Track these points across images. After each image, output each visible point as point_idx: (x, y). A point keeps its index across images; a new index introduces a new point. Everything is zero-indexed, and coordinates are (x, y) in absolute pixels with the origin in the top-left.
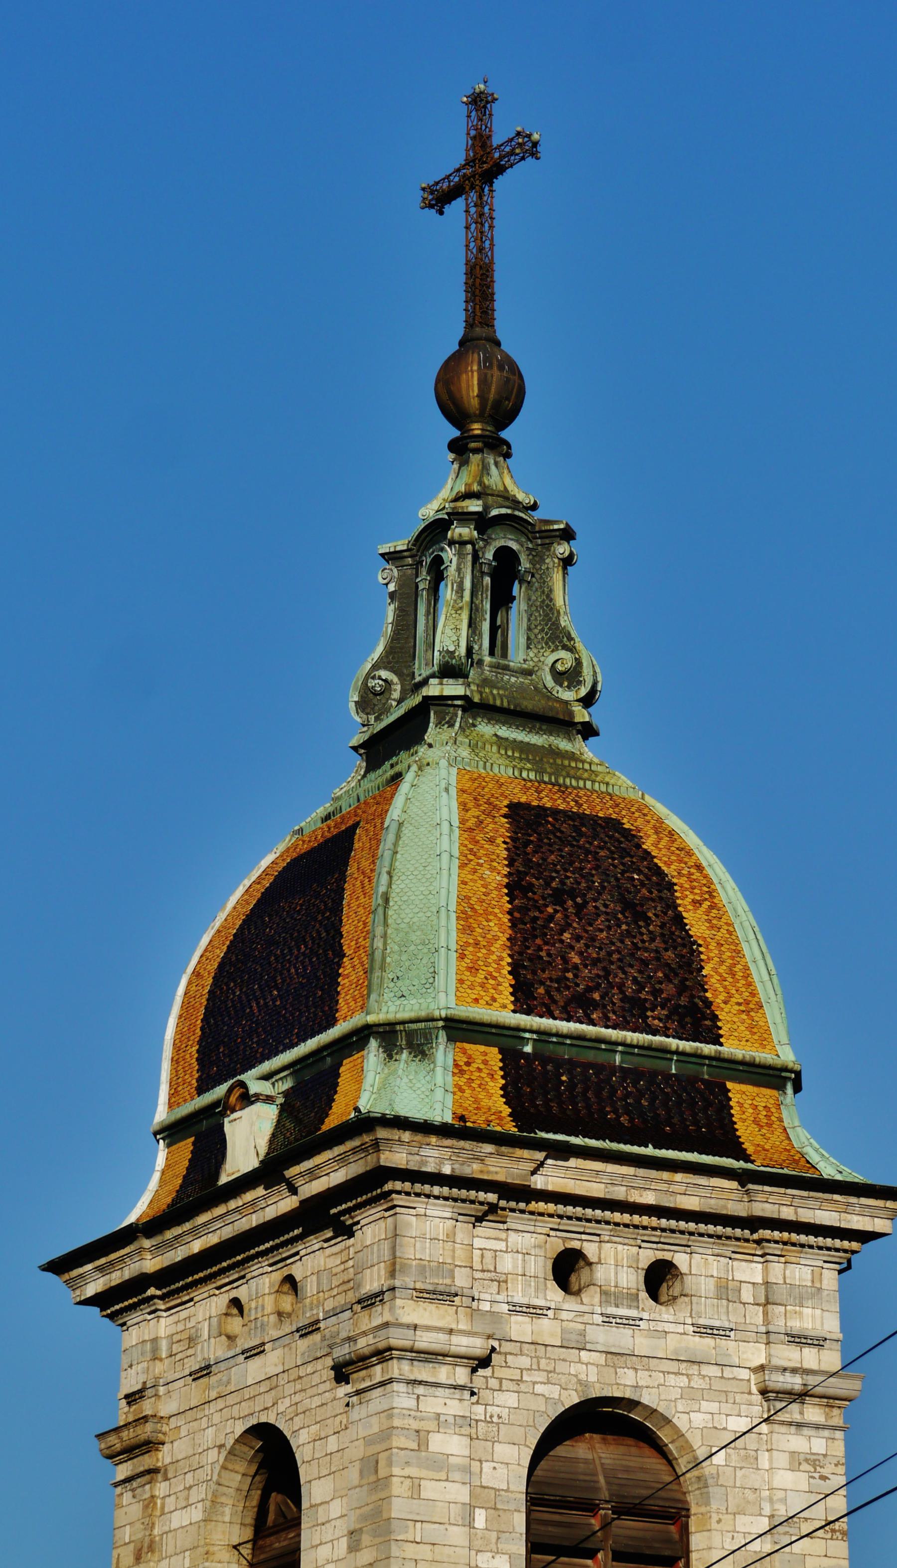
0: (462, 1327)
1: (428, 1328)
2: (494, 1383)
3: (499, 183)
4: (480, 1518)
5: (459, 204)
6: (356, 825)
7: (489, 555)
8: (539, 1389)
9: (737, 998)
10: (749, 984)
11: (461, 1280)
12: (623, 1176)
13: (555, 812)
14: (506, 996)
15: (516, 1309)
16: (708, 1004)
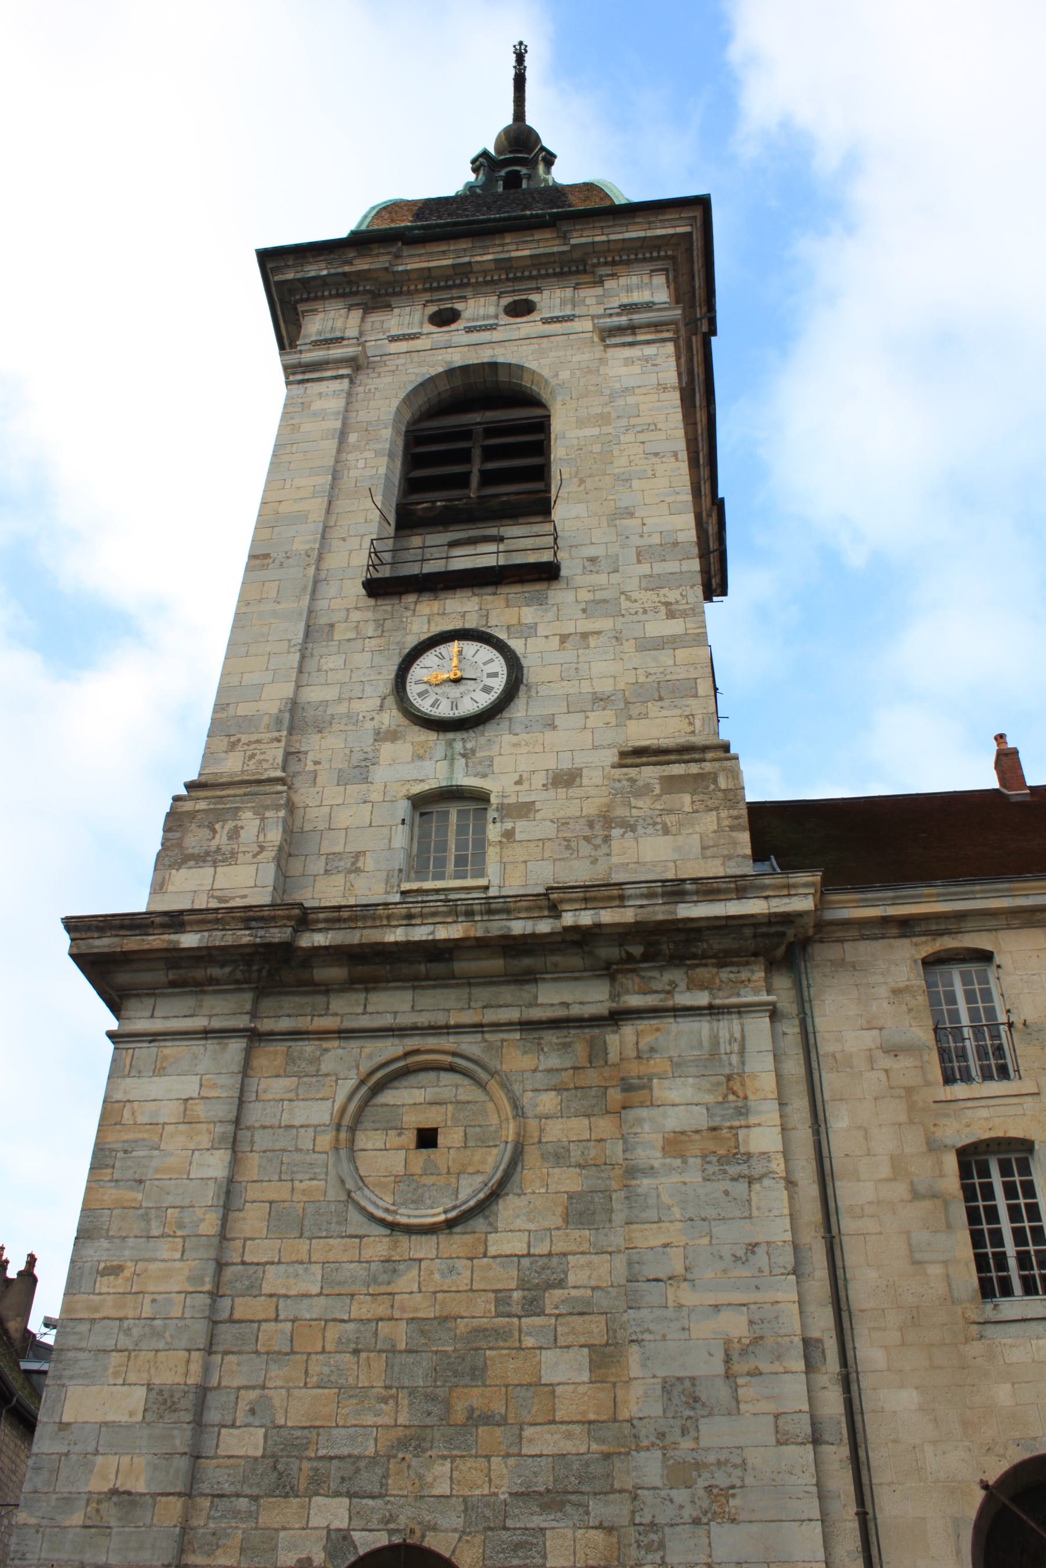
12: (465, 250)
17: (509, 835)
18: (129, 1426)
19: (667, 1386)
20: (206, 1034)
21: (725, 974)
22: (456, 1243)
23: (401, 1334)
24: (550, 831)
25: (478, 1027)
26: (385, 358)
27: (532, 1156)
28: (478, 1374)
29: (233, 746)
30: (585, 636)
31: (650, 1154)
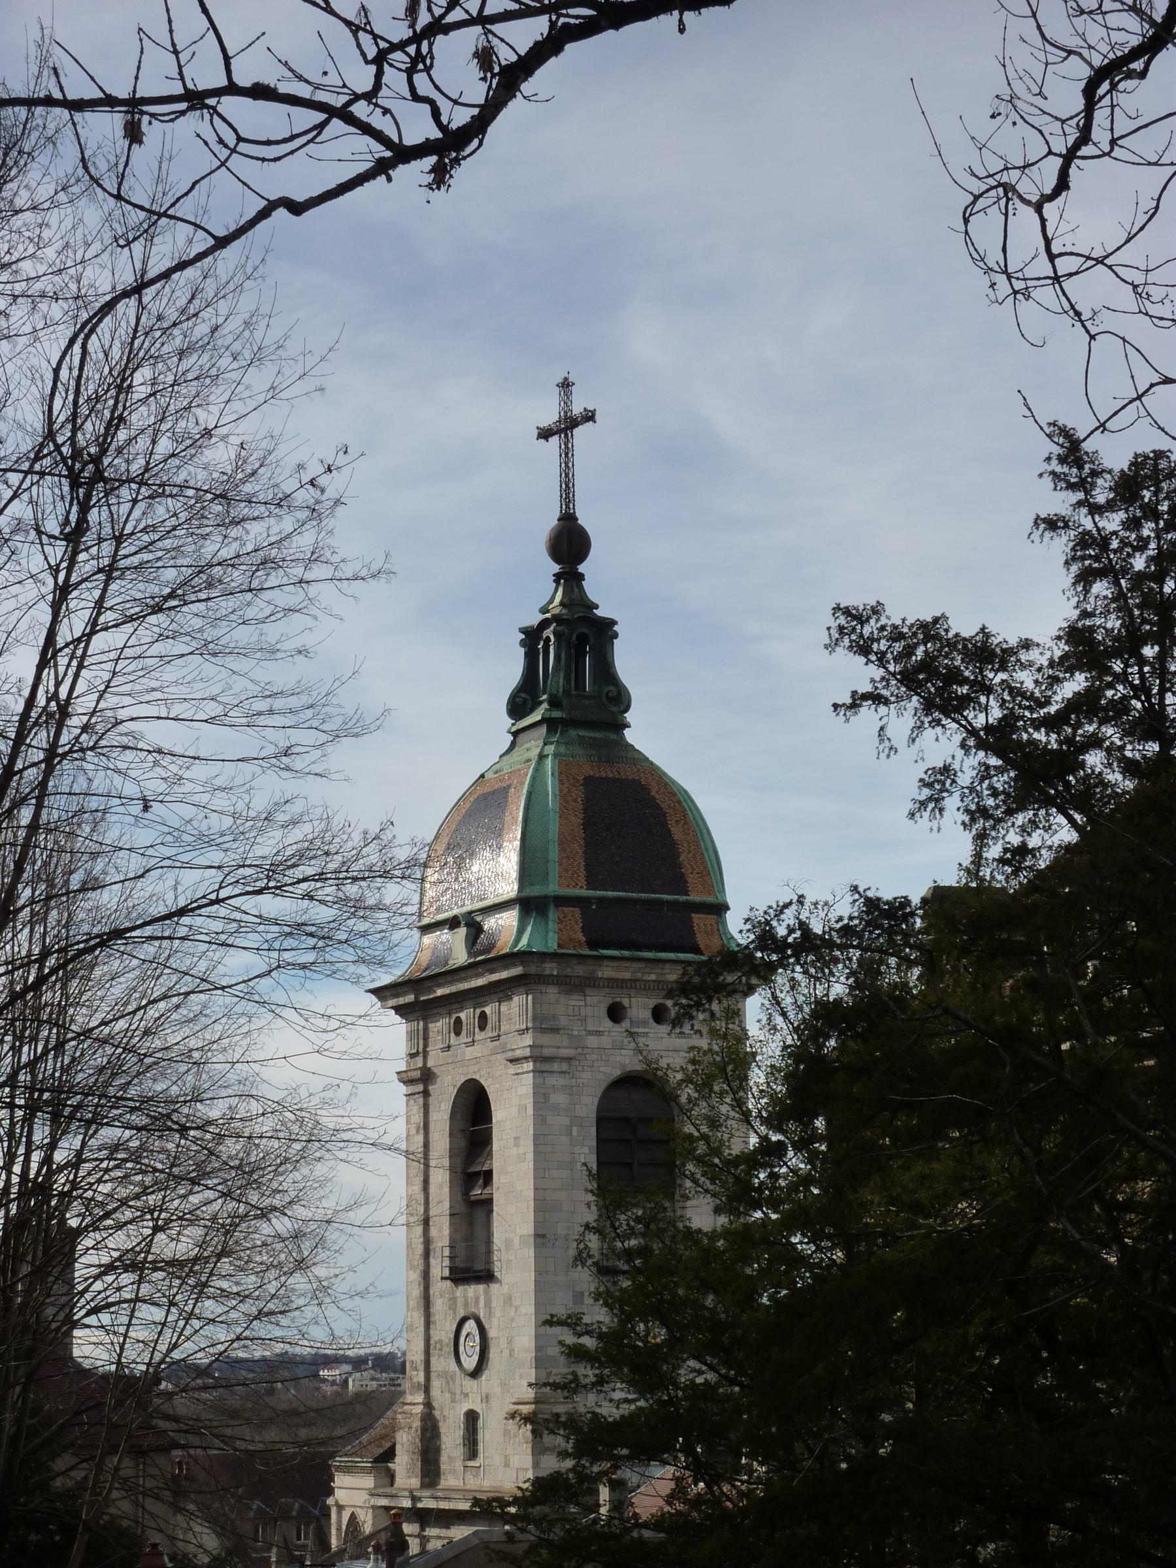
0: (564, 1044)
1: (548, 1047)
2: (580, 1068)
3: (575, 431)
4: (575, 1131)
5: (554, 440)
6: (509, 786)
7: (574, 638)
8: (602, 1069)
9: (697, 870)
10: (703, 863)
11: (563, 1021)
13: (607, 779)
14: (583, 882)
15: (590, 1033)
16: (683, 875)
26: (586, 1051)
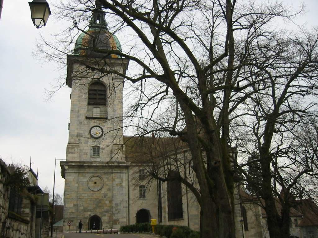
17: (102, 152)
18: (72, 207)
19: (115, 204)
20: (74, 173)
21: (122, 169)
22: (99, 192)
23: (94, 200)
24: (106, 152)
25: (100, 173)
27: (105, 185)
28: (100, 203)
29: (72, 138)
30: (110, 128)
31: (115, 185)
